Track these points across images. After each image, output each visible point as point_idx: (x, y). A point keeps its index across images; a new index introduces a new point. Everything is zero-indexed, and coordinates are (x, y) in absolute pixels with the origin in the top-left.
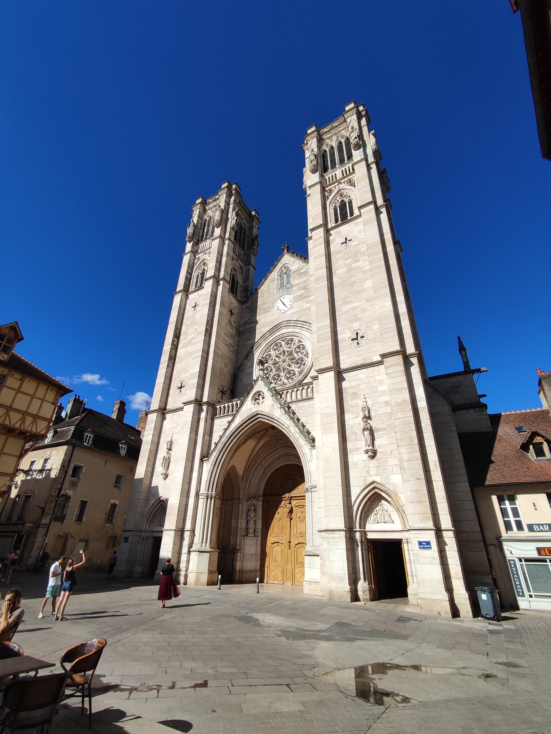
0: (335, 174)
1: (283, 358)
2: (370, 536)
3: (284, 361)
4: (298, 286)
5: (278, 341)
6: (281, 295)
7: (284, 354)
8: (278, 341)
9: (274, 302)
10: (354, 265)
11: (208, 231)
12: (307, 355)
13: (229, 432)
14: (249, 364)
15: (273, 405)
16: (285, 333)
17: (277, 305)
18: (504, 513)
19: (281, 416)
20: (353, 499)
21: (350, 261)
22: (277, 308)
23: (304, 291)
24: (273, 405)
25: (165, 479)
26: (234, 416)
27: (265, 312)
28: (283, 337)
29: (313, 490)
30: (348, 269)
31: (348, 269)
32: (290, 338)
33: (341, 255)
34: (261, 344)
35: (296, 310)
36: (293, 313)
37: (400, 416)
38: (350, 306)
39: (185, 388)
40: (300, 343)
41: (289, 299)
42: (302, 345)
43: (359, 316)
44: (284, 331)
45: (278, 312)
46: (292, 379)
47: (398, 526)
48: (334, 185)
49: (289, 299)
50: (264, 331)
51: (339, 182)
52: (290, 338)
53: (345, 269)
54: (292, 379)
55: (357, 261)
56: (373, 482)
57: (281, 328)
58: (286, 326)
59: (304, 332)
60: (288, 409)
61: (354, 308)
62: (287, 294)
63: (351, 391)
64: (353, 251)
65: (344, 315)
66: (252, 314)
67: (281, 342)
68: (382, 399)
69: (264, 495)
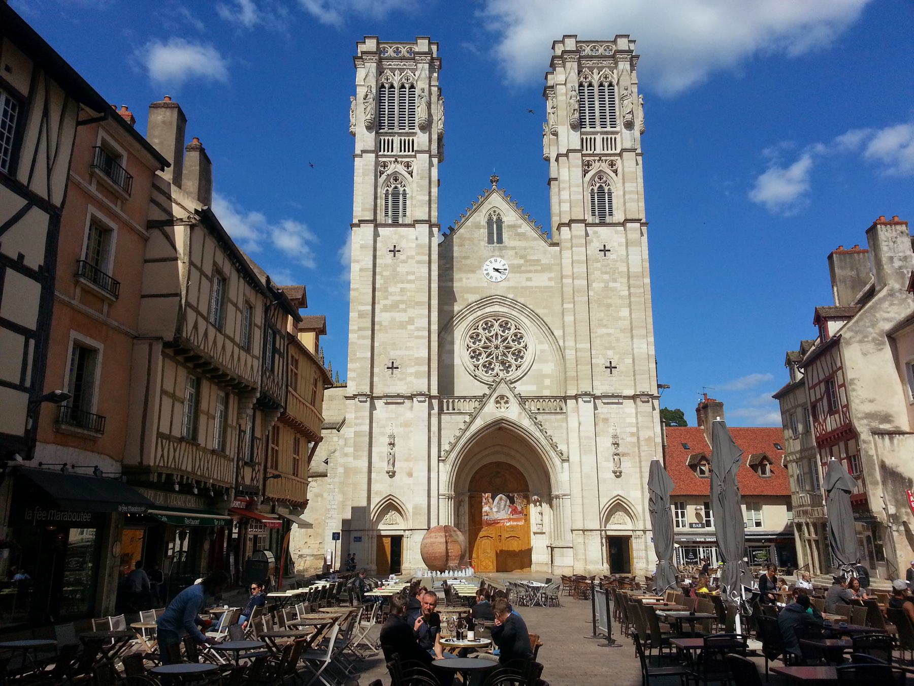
0: (595, 139)
1: (495, 343)
2: (609, 533)
3: (497, 347)
4: (514, 251)
5: (489, 319)
6: (491, 254)
7: (497, 338)
8: (489, 319)
9: (482, 260)
10: (611, 285)
11: (391, 114)
12: (525, 347)
13: (468, 434)
14: (449, 339)
15: (521, 413)
16: (499, 312)
17: (485, 267)
18: (677, 513)
19: (530, 426)
20: (601, 507)
21: (606, 277)
22: (487, 272)
23: (522, 261)
24: (521, 413)
25: (391, 477)
26: (474, 418)
27: (469, 271)
28: (496, 316)
29: (564, 497)
30: (606, 287)
31: (606, 287)
32: (504, 319)
33: (598, 265)
34: (465, 316)
35: (511, 284)
36: (509, 288)
37: (646, 449)
38: (605, 331)
39: (399, 370)
40: (517, 330)
41: (503, 265)
42: (520, 333)
43: (613, 345)
44: (497, 308)
45: (488, 278)
46: (508, 372)
47: (630, 526)
48: (593, 158)
49: (503, 265)
50: (468, 300)
51: (600, 158)
52: (504, 319)
53: (602, 285)
54: (508, 372)
55: (615, 281)
56: (618, 495)
57: (493, 302)
58: (500, 302)
59: (522, 318)
60: (533, 417)
61: (609, 335)
62: (502, 257)
63: (602, 416)
64: (611, 266)
65: (599, 339)
66: (447, 266)
67: (493, 321)
68: (628, 430)
69: (469, 491)
